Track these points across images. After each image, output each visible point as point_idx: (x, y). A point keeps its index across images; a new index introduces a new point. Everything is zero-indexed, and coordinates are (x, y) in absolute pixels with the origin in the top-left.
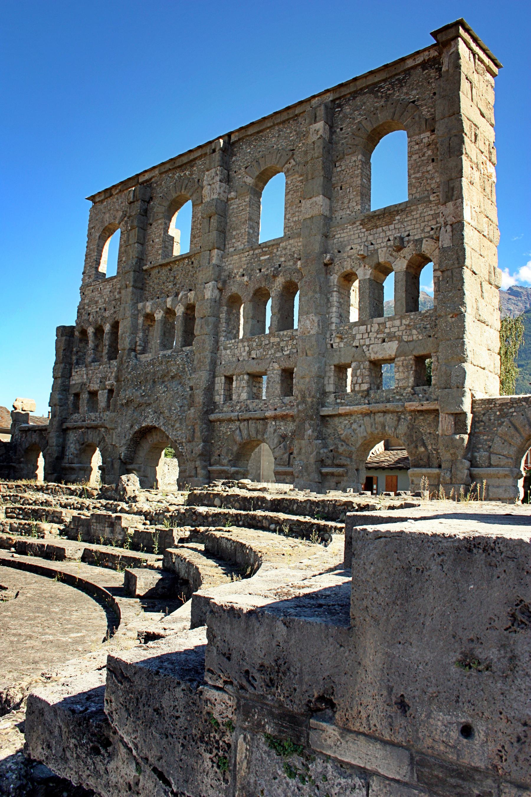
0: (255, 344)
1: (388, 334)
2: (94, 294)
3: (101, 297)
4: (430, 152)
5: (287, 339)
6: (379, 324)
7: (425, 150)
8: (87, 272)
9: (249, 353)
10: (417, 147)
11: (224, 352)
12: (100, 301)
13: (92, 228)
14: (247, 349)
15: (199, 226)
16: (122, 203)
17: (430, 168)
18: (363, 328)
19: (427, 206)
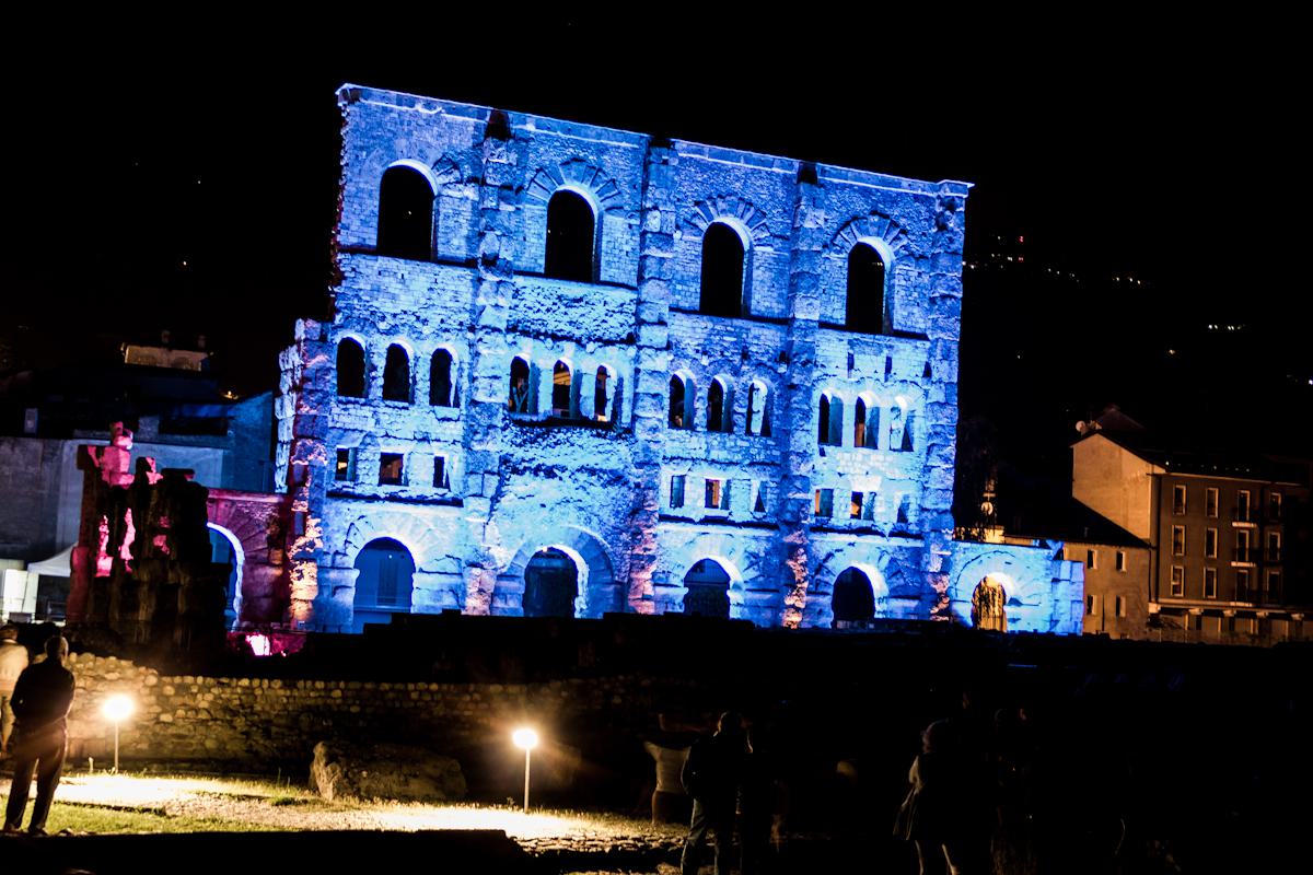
0: (715, 443)
1: (872, 468)
2: (386, 280)
3: (408, 290)
4: (916, 294)
5: (758, 446)
6: (864, 455)
7: (912, 289)
8: (353, 228)
9: (708, 451)
10: (904, 283)
11: (669, 444)
12: (403, 297)
13: (362, 148)
14: (705, 447)
15: (617, 252)
16: (440, 135)
17: (916, 310)
18: (847, 456)
19: (914, 351)
